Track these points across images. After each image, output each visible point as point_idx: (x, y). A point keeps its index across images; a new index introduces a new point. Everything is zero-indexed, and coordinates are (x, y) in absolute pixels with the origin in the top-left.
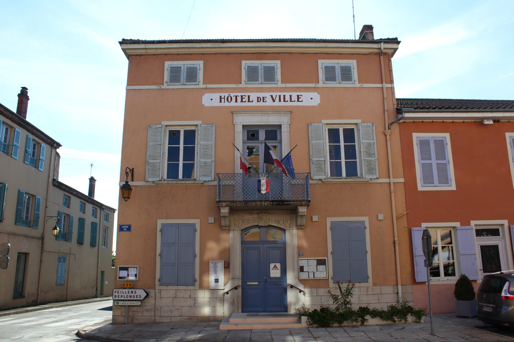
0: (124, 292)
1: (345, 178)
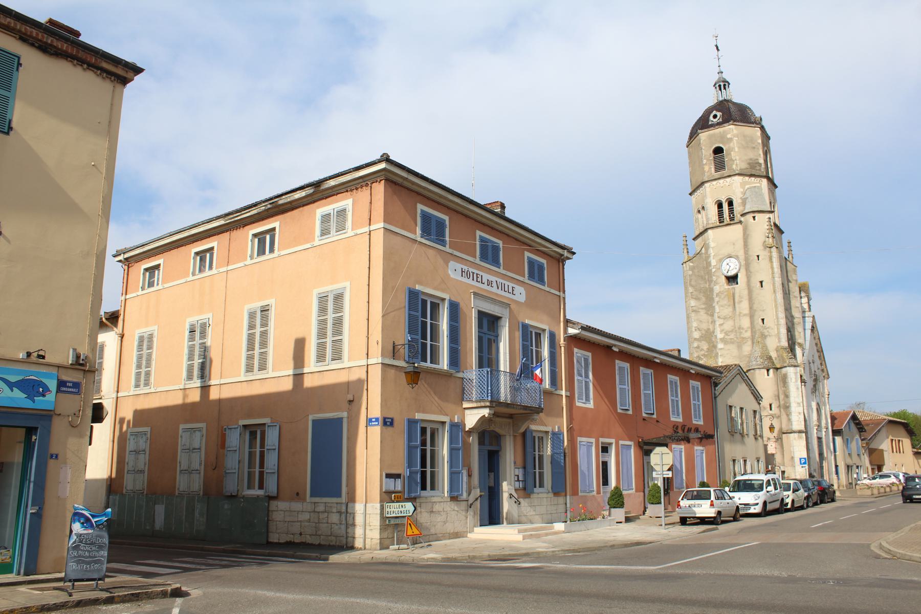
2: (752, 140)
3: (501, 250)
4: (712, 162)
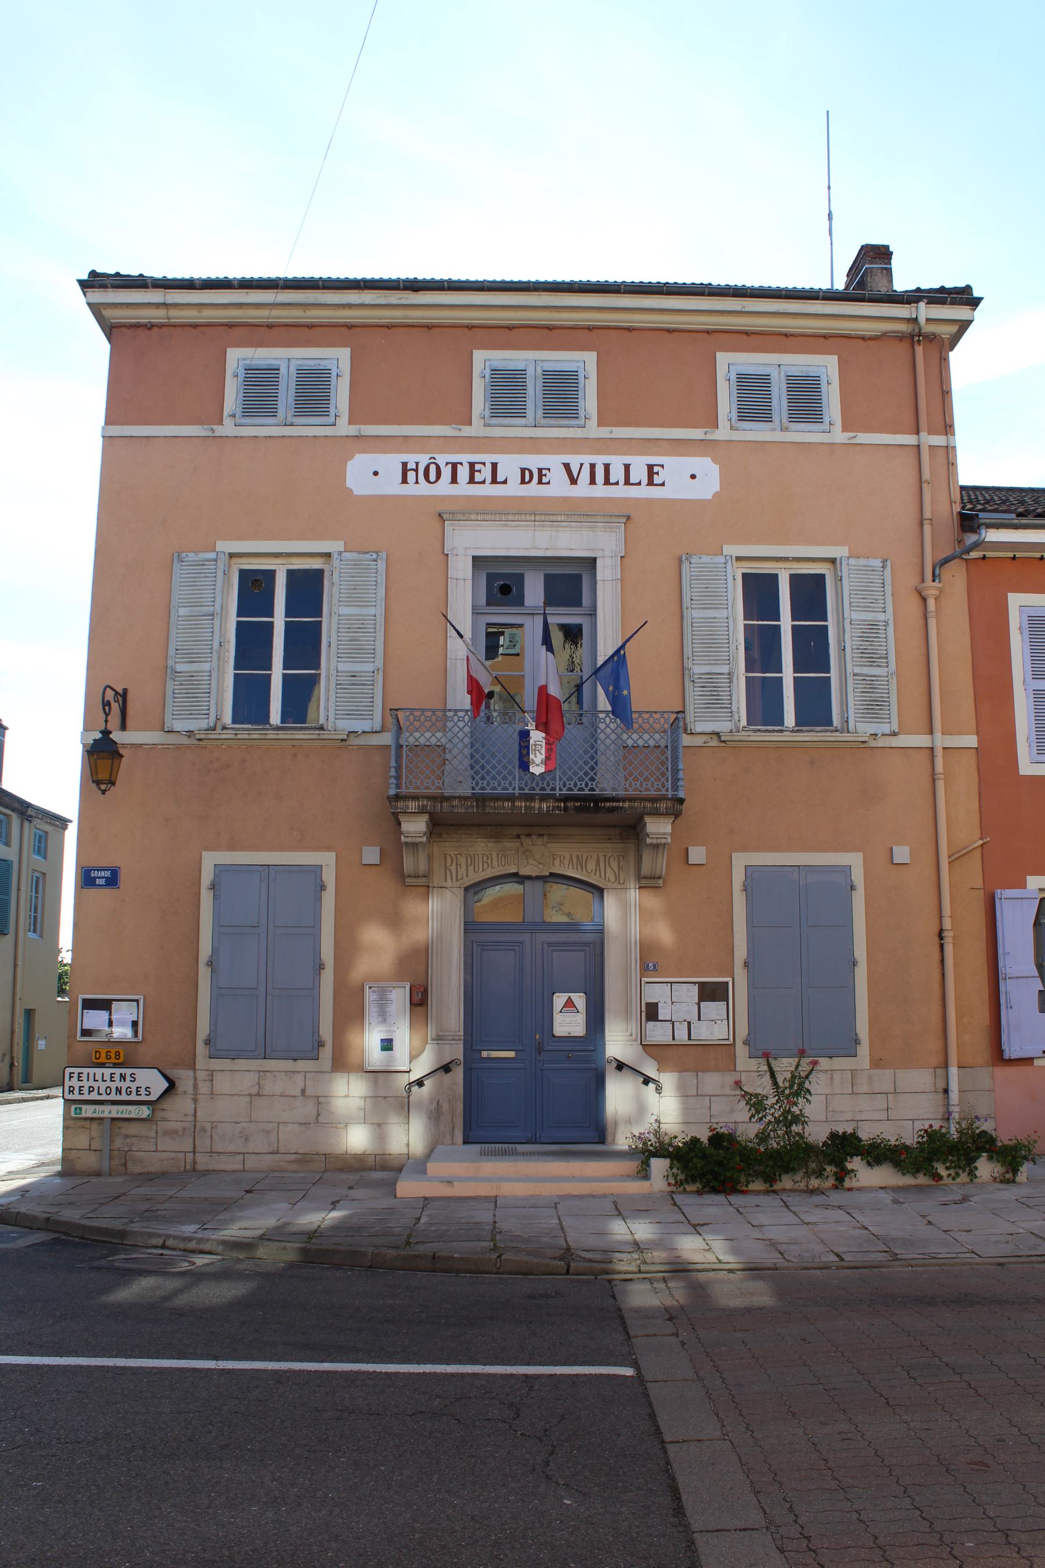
1: (793, 731)
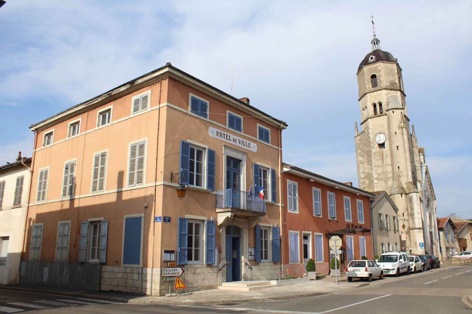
0: (170, 270)
2: (392, 71)
3: (242, 121)
4: (371, 82)
